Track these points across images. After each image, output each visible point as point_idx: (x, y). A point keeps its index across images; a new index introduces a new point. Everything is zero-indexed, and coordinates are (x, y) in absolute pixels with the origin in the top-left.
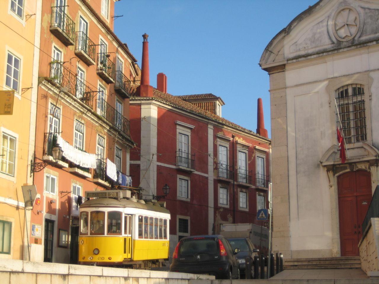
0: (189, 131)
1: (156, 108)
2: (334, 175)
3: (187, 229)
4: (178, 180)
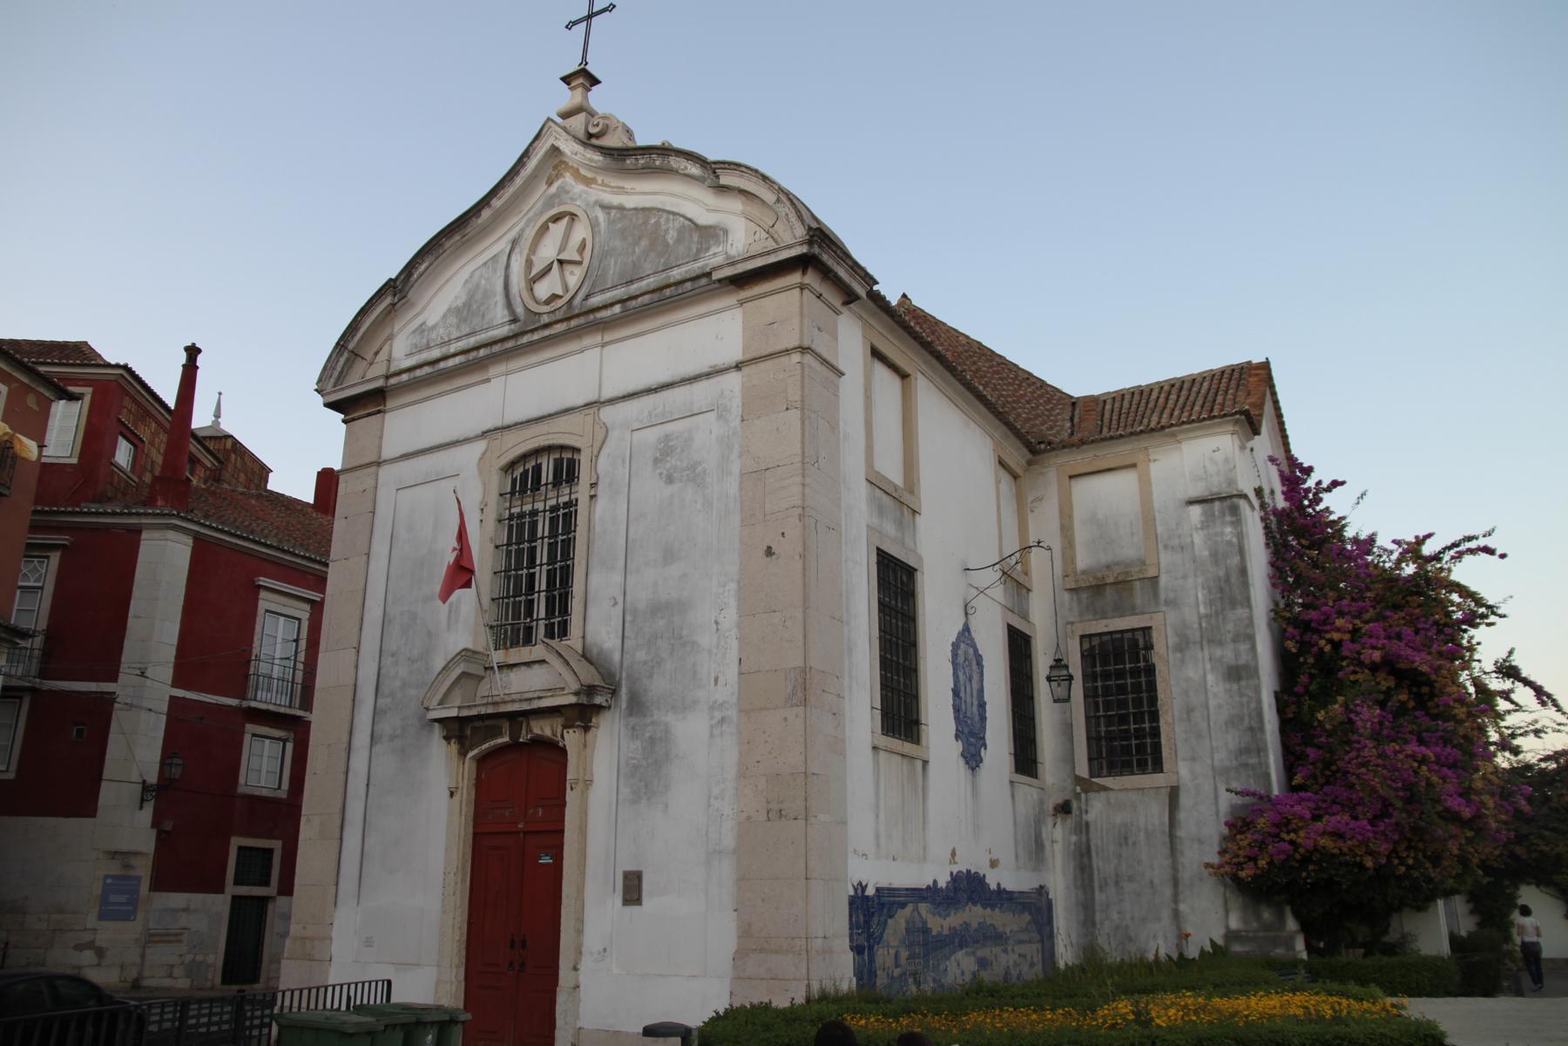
0: (307, 607)
1: (190, 541)
2: (463, 753)
3: (269, 875)
4: (247, 737)
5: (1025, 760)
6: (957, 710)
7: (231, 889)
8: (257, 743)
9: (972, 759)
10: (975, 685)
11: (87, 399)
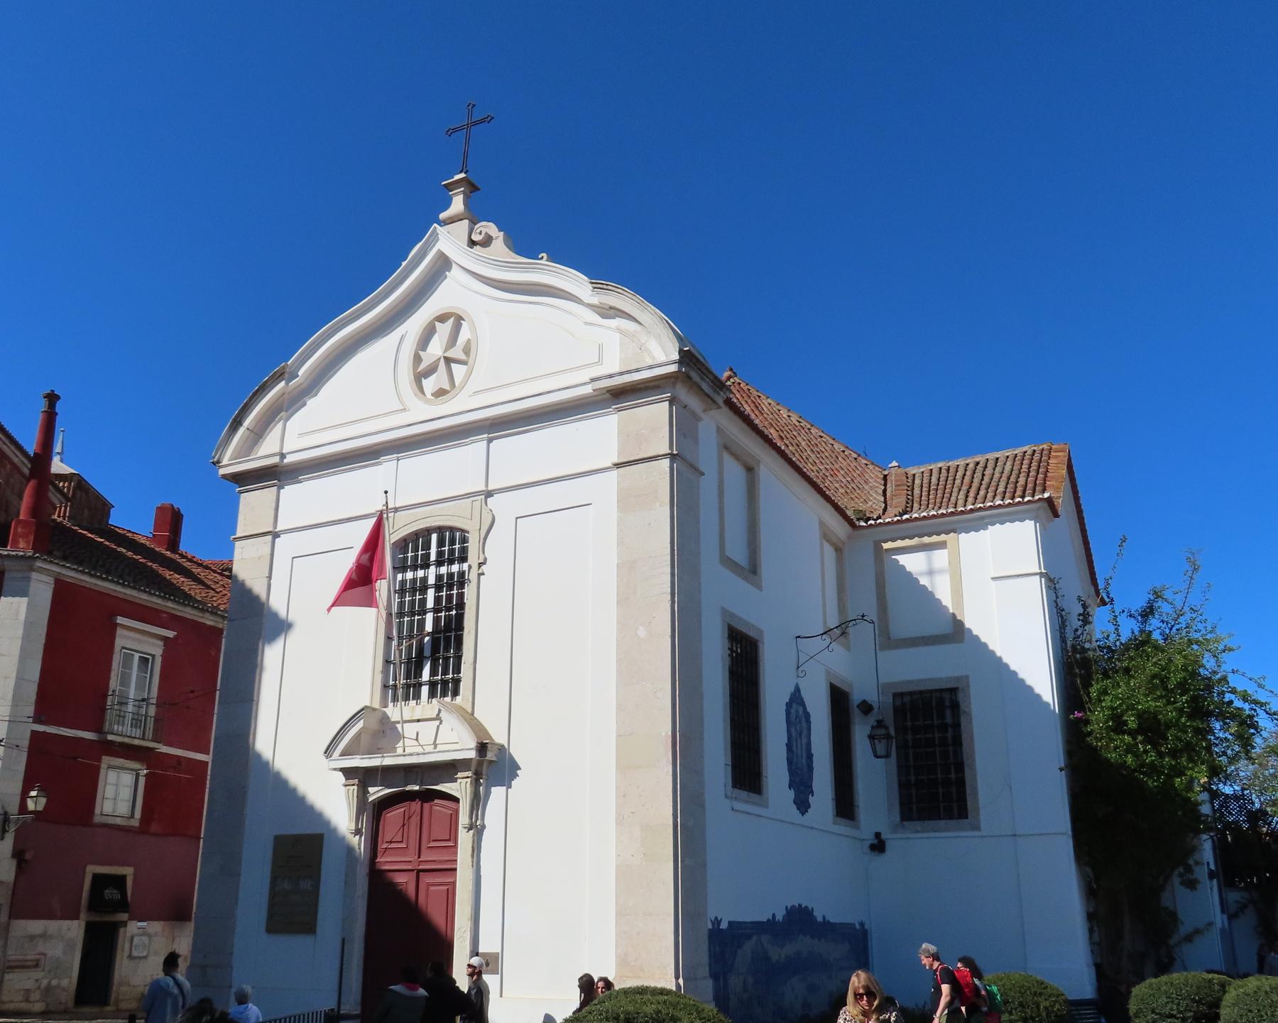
1: (51, 580)
5: (845, 806)
6: (790, 762)
7: (83, 915)
9: (802, 805)
10: (804, 741)
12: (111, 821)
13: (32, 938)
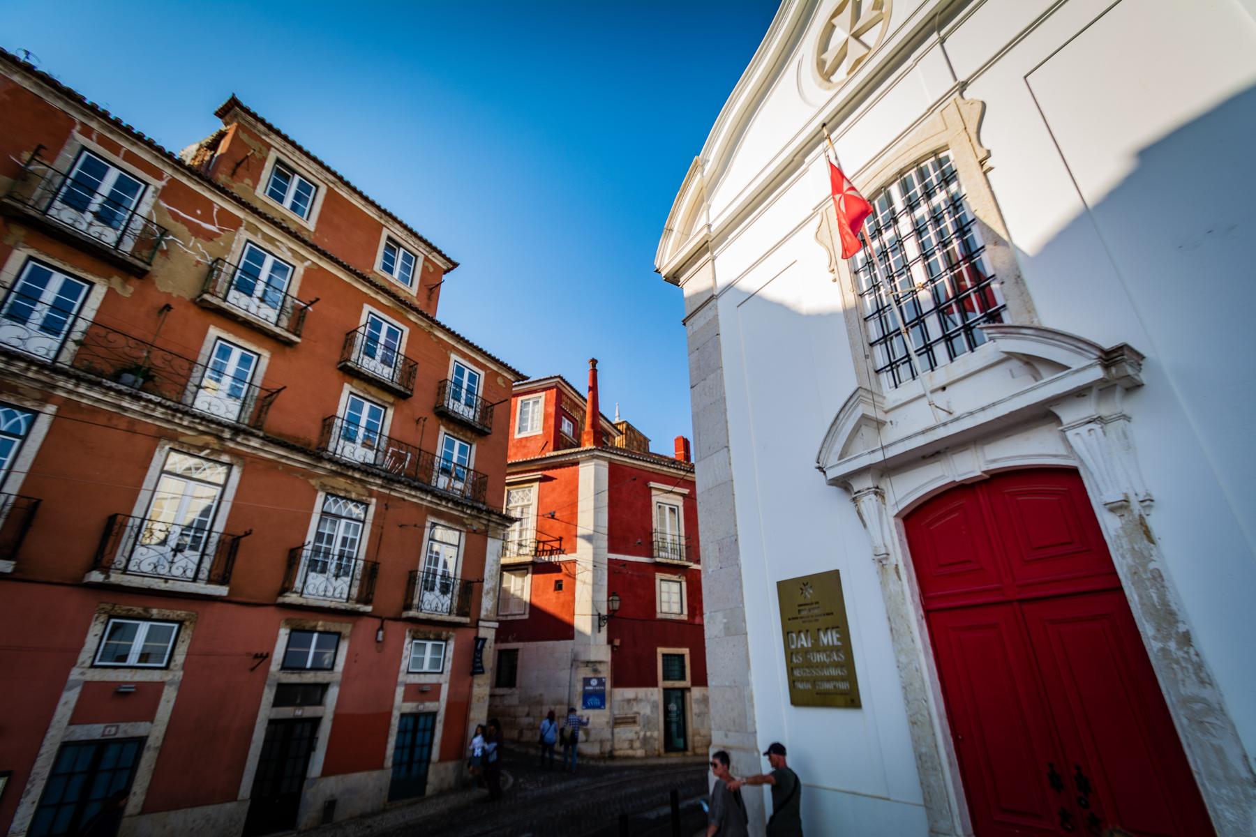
1: (606, 464)
4: (658, 581)
7: (661, 683)
8: (664, 585)
11: (542, 401)
12: (669, 617)
13: (629, 701)
